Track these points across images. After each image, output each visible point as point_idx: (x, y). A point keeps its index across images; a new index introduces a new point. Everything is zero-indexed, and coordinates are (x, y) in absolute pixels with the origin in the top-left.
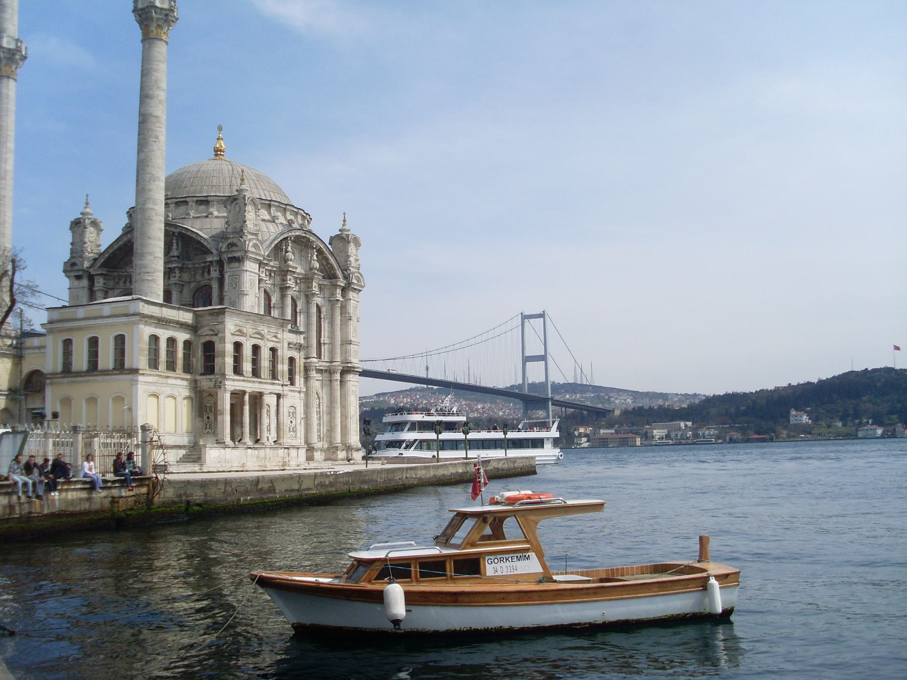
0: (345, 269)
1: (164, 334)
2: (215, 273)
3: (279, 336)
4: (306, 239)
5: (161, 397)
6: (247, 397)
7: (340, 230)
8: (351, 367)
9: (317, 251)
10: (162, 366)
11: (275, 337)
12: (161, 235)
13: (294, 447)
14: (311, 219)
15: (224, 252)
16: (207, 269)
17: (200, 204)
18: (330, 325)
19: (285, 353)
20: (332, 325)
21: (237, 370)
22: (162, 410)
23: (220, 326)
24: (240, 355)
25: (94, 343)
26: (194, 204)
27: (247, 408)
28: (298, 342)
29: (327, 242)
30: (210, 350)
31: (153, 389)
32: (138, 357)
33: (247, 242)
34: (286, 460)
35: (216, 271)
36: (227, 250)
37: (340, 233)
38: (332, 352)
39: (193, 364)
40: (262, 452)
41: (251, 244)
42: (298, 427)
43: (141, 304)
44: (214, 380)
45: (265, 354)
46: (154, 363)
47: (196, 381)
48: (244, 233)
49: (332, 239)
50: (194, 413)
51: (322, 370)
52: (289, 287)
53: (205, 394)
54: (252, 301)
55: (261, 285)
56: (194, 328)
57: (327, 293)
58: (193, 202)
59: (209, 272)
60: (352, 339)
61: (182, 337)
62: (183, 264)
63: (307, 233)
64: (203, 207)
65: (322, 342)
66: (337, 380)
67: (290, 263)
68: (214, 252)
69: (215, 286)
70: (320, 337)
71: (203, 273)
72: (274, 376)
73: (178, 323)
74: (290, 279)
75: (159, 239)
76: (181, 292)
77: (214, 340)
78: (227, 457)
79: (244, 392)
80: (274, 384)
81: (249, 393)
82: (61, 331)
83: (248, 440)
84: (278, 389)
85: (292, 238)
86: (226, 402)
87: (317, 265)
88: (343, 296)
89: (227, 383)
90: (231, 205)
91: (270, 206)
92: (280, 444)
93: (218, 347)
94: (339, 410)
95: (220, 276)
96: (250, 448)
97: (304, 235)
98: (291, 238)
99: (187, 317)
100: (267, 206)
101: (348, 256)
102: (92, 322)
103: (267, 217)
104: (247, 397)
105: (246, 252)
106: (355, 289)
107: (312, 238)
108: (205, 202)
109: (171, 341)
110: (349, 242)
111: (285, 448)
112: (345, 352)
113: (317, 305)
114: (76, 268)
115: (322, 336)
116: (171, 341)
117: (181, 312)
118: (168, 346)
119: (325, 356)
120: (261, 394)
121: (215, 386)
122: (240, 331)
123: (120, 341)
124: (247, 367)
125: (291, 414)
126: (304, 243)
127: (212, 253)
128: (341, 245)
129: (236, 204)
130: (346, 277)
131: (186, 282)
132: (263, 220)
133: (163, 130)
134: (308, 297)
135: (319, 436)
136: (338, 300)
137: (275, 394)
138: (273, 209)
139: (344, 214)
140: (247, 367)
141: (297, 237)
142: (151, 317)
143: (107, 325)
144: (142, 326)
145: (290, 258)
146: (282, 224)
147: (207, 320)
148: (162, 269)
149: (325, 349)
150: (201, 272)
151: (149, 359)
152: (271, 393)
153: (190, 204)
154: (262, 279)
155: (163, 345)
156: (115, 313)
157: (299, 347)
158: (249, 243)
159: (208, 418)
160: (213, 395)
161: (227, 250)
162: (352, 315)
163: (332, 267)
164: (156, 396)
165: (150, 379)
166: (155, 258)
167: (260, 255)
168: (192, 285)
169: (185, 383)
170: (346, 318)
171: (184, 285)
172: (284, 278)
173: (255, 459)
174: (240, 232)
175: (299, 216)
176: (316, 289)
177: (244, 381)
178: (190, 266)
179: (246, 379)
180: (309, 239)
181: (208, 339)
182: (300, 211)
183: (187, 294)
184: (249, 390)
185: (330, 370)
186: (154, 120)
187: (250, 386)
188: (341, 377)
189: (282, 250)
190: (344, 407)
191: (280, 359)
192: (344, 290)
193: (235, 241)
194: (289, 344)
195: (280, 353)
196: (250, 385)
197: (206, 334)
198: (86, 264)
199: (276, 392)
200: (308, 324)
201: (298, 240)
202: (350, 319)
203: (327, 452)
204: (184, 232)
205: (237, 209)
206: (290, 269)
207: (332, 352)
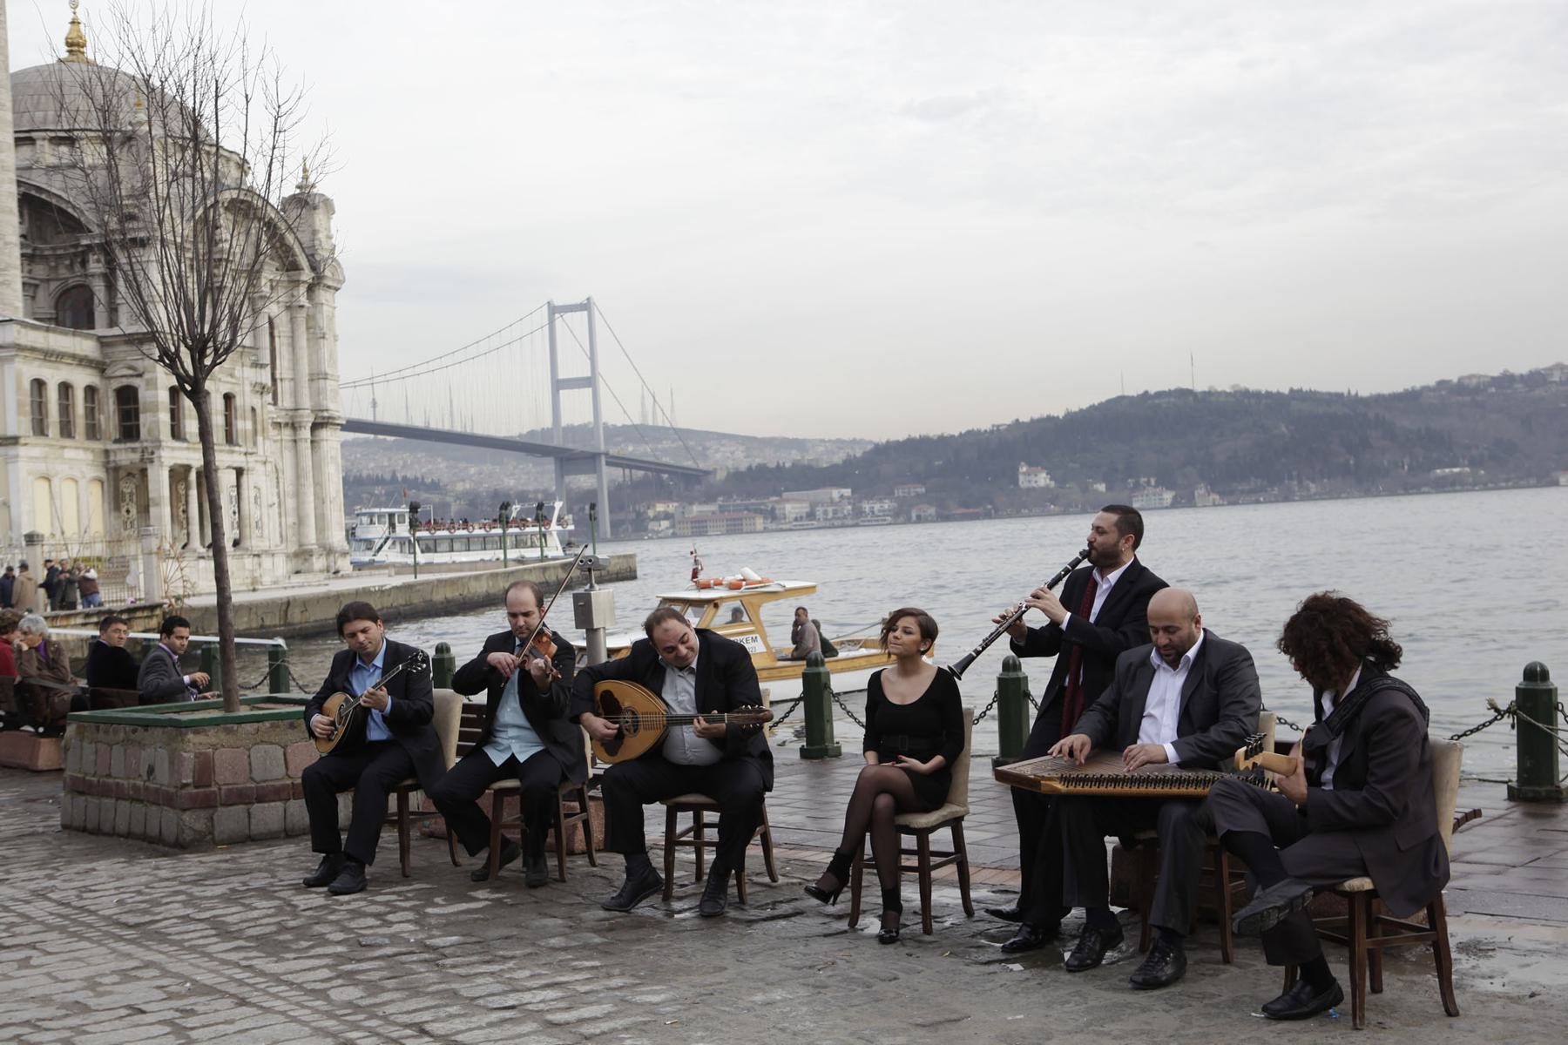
1: (53, 376)
2: (96, 266)
3: (237, 373)
4: (245, 204)
5: (55, 481)
7: (298, 187)
8: (329, 418)
10: (53, 428)
11: (232, 376)
13: (266, 552)
16: (82, 257)
17: (59, 145)
18: (291, 349)
20: (294, 349)
21: (177, 433)
24: (178, 407)
26: (46, 143)
28: (259, 381)
31: (41, 467)
34: (257, 574)
35: (98, 261)
37: (298, 191)
38: (295, 394)
39: (100, 426)
44: (140, 450)
46: (40, 428)
47: (107, 452)
50: (106, 505)
51: (280, 424)
53: (122, 473)
56: (101, 367)
58: (44, 139)
59: (84, 263)
60: (329, 371)
61: (82, 378)
62: (35, 249)
64: (64, 149)
65: (278, 376)
66: (306, 440)
68: (96, 230)
69: (99, 289)
71: (71, 266)
73: (74, 356)
75: (11, 212)
76: (33, 298)
77: (136, 385)
80: (233, 452)
81: (197, 469)
84: (239, 460)
88: (310, 298)
92: (247, 549)
93: (144, 395)
94: (312, 489)
96: (203, 558)
99: (84, 345)
101: (314, 232)
106: (329, 287)
109: (65, 388)
111: (254, 555)
112: (317, 394)
116: (65, 388)
119: (286, 401)
121: (142, 460)
126: (246, 208)
127: (90, 231)
131: (42, 280)
136: (302, 307)
141: (232, 201)
142: (33, 349)
150: (67, 262)
151: (33, 419)
152: (228, 467)
153: (39, 143)
155: (52, 395)
159: (128, 511)
160: (141, 474)
162: (325, 330)
165: (36, 452)
166: (6, 244)
168: (53, 285)
169: (90, 456)
170: (317, 335)
171: (36, 286)
177: (188, 449)
178: (46, 253)
179: (191, 446)
181: (125, 382)
185: (293, 424)
188: (312, 435)
190: (318, 484)
191: (239, 412)
192: (311, 289)
195: (238, 401)
199: (235, 465)
202: (324, 338)
203: (294, 561)
204: (33, 193)
207: (295, 394)
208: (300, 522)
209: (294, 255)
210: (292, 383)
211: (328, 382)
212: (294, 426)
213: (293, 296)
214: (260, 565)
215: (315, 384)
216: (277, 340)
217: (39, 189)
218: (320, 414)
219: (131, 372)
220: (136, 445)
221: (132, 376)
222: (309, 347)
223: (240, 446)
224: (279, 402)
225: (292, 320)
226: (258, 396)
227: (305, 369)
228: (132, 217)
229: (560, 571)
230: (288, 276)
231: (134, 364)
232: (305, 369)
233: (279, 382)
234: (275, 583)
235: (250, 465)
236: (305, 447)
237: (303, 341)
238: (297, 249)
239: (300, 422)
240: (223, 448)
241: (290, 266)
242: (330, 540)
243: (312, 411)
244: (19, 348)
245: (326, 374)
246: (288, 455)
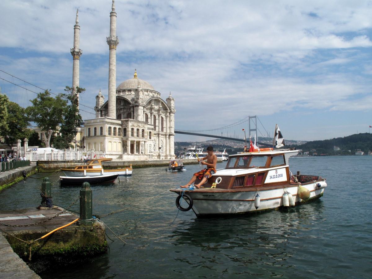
1: (113, 127)
2: (132, 110)
3: (145, 126)
6: (135, 142)
12: (115, 101)
16: (130, 109)
19: (147, 131)
21: (132, 135)
22: (112, 146)
23: (127, 124)
25: (95, 129)
29: (165, 100)
30: (125, 130)
31: (110, 140)
32: (106, 132)
40: (140, 156)
43: (106, 119)
45: (141, 131)
46: (110, 134)
54: (141, 118)
56: (121, 125)
61: (118, 127)
72: (143, 136)
76: (124, 115)
78: (129, 157)
79: (134, 141)
82: (87, 126)
84: (144, 140)
86: (129, 144)
87: (161, 106)
89: (129, 138)
91: (148, 91)
93: (127, 129)
99: (120, 122)
101: (171, 104)
102: (95, 124)
103: (147, 94)
104: (135, 142)
107: (160, 99)
108: (130, 90)
109: (115, 128)
110: (171, 100)
113: (162, 117)
114: (97, 109)
116: (115, 128)
117: (118, 121)
118: (119, 130)
120: (139, 142)
121: (126, 140)
122: (133, 125)
123: (101, 128)
124: (135, 134)
128: (169, 101)
132: (146, 95)
133: (115, 73)
140: (135, 134)
143: (98, 124)
144: (106, 125)
146: (151, 96)
147: (125, 123)
148: (115, 109)
149: (165, 129)
152: (142, 141)
155: (112, 129)
156: (100, 121)
163: (166, 107)
164: (111, 142)
165: (109, 138)
168: (127, 113)
173: (137, 158)
174: (138, 99)
175: (156, 94)
181: (125, 127)
183: (125, 115)
184: (136, 140)
186: (112, 70)
187: (136, 139)
190: (170, 145)
192: (170, 113)
197: (124, 126)
198: (100, 107)
201: (155, 100)
217: (125, 98)
220: (126, 137)
227: (168, 126)
232: (168, 126)
236: (168, 139)
237: (168, 122)
238: (167, 107)
244: (107, 122)
246: (165, 140)
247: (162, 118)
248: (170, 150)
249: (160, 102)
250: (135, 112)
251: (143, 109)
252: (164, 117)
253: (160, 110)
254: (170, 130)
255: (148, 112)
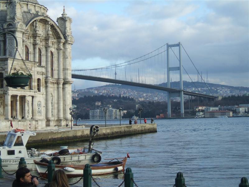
0: (64, 34)
6: (18, 98)
7: (62, 15)
8: (67, 81)
9: (51, 26)
14: (47, 10)
15: (6, 28)
18: (58, 61)
23: (6, 66)
27: (18, 103)
29: (55, 21)
33: (17, 24)
34: (37, 126)
36: (7, 27)
37: (62, 16)
38: (59, 74)
41: (19, 25)
42: (42, 110)
44: (3, 91)
48: (15, 19)
49: (58, 19)
52: (37, 44)
55: (24, 43)
57: (56, 46)
60: (68, 68)
63: (46, 17)
65: (54, 69)
67: (37, 32)
70: (53, 67)
74: (38, 40)
79: (17, 96)
80: (31, 91)
81: (19, 96)
83: (19, 117)
84: (32, 93)
85: (39, 20)
86: (9, 100)
87: (50, 33)
89: (9, 92)
90: (9, 6)
91: (27, 4)
92: (34, 119)
95: (4, 39)
96: (20, 121)
97: (44, 19)
98: (38, 20)
100: (26, 5)
104: (18, 98)
105: (16, 28)
106: (69, 44)
107: (48, 20)
110: (66, 21)
111: (36, 121)
113: (51, 51)
115: (54, 66)
119: (56, 76)
125: (39, 105)
126: (45, 21)
128: (63, 22)
129: (12, 5)
130: (65, 38)
132: (24, 12)
134: (47, 47)
135: (52, 115)
136: (61, 49)
137: (31, 96)
138: (29, 5)
139: (64, 7)
145: (37, 30)
149: (55, 73)
154: (24, 41)
157: (43, 74)
158: (18, 24)
161: (7, 27)
162: (68, 56)
163: (58, 33)
167: (23, 29)
172: (35, 39)
176: (50, 44)
177: (17, 90)
180: (46, 21)
182: (42, 7)
184: (19, 95)
188: (63, 86)
189: (33, 26)
190: (64, 100)
191: (33, 80)
192: (64, 44)
193: (11, 23)
194: (38, 72)
196: (20, 92)
200: (47, 61)
205: (12, 8)
206: (38, 35)
207: (59, 74)
208: (59, 111)
209: (59, 34)
210: (58, 71)
211: (68, 71)
212: (58, 84)
213: (59, 46)
214: (38, 123)
215: (64, 72)
216: (54, 58)
218: (65, 80)
219: (2, 69)
221: (2, 70)
222: (63, 61)
223: (33, 90)
224: (54, 77)
225: (58, 53)
226: (42, 75)
228: (10, 25)
229: (126, 128)
230: (58, 40)
231: (2, 67)
233: (54, 71)
234: (42, 129)
235: (36, 95)
238: (60, 33)
239: (59, 82)
240: (28, 90)
241: (59, 38)
242: (67, 117)
243: (63, 79)
245: (68, 69)
246: (56, 92)
247: (52, 53)
248: (64, 110)
249: (48, 24)
250: (7, 42)
251: (22, 37)
252: (53, 50)
253: (48, 39)
254: (65, 74)
255: (29, 43)
